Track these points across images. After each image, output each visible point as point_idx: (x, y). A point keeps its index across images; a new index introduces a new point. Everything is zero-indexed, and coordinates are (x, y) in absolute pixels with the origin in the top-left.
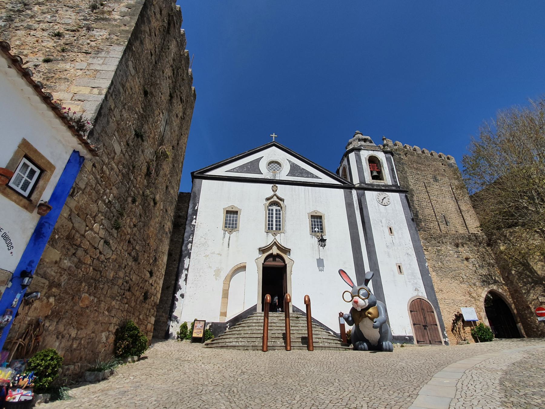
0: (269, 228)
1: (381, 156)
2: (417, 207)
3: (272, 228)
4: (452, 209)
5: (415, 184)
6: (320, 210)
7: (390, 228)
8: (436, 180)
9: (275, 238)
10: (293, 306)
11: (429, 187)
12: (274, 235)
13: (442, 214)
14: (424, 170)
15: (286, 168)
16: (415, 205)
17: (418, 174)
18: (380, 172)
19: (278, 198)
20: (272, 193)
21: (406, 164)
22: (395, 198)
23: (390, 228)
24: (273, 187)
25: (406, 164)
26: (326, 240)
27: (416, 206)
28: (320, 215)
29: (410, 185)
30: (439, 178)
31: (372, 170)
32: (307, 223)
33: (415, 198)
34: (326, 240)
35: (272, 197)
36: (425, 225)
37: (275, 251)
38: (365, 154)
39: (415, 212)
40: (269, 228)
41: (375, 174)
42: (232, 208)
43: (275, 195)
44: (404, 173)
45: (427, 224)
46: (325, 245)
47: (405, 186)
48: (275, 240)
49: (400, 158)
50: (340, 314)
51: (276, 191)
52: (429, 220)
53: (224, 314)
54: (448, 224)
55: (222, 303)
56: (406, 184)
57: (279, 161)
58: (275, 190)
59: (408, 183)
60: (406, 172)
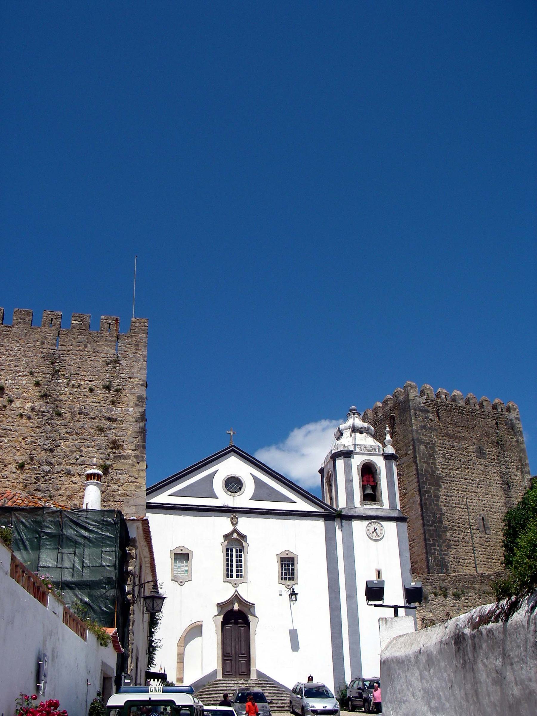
0: (228, 576)
1: (380, 463)
2: (443, 507)
3: (232, 576)
4: (499, 504)
5: (446, 466)
6: (294, 549)
7: (379, 572)
8: (481, 453)
9: (236, 591)
10: (257, 670)
11: (468, 468)
12: (235, 585)
13: (480, 515)
14: (464, 439)
15: (249, 488)
16: (440, 504)
17: (453, 447)
18: (375, 487)
19: (239, 534)
20: (230, 528)
21: (436, 430)
22: (391, 528)
23: (379, 572)
24: (232, 518)
25: (436, 430)
26: (297, 594)
27: (442, 504)
28: (292, 556)
29: (436, 468)
30: (487, 450)
31: (365, 483)
32: (275, 568)
33: (442, 492)
34: (297, 594)
35: (232, 533)
36: (451, 536)
37: (236, 607)
38: (357, 461)
39: (438, 516)
40: (229, 575)
41: (369, 491)
42: (182, 550)
43: (235, 531)
44: (431, 448)
45: (454, 535)
46: (296, 600)
47: (428, 471)
48: (236, 593)
49: (427, 418)
50: (309, 678)
51: (237, 523)
52: (459, 527)
53: (180, 680)
54: (487, 531)
55: (177, 667)
56: (432, 468)
57: (239, 477)
58: (235, 523)
59: (435, 464)
60: (432, 448)
